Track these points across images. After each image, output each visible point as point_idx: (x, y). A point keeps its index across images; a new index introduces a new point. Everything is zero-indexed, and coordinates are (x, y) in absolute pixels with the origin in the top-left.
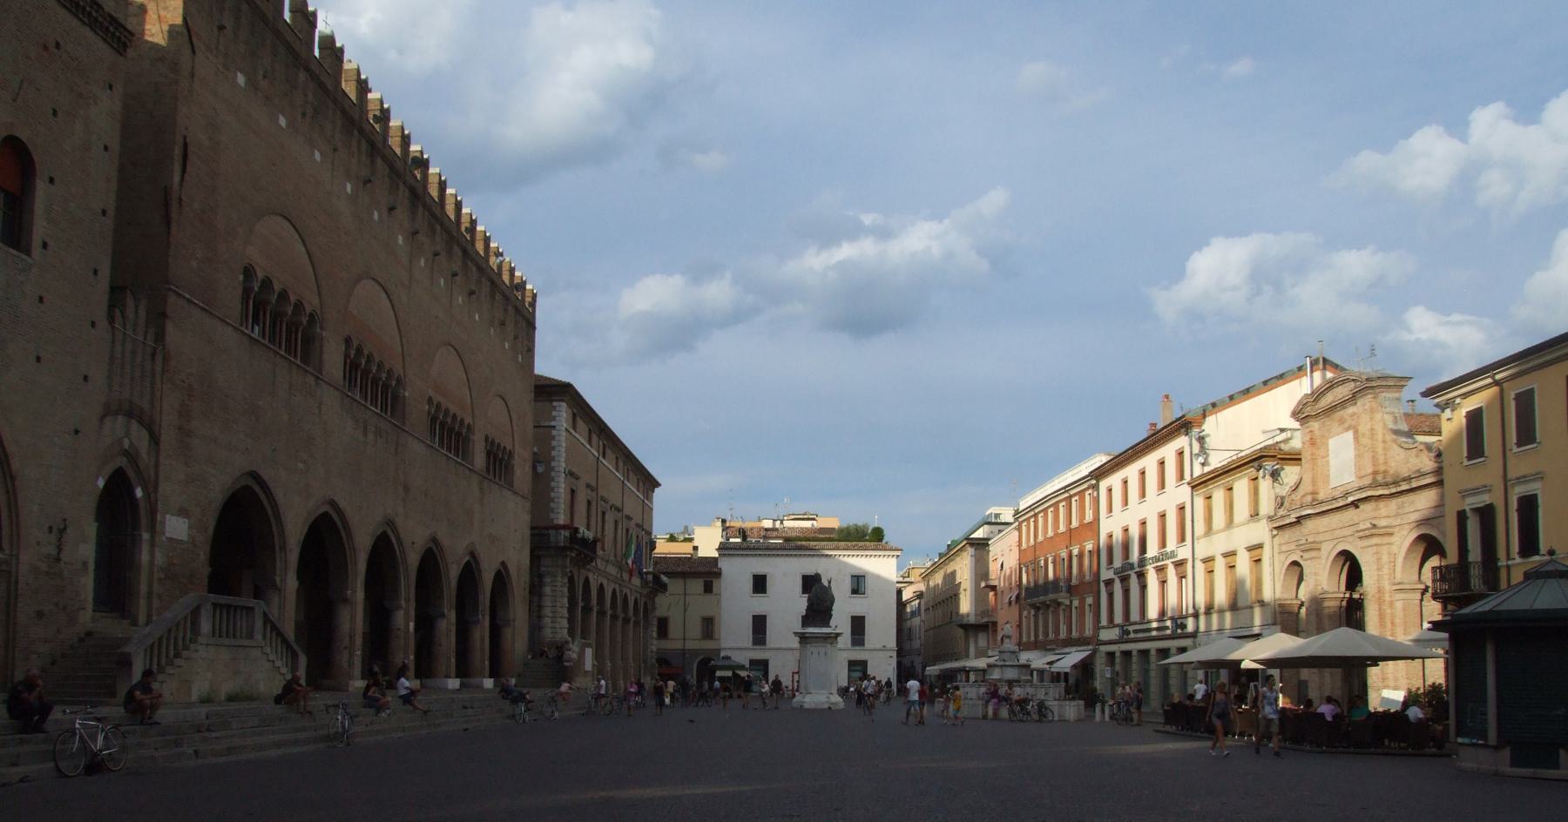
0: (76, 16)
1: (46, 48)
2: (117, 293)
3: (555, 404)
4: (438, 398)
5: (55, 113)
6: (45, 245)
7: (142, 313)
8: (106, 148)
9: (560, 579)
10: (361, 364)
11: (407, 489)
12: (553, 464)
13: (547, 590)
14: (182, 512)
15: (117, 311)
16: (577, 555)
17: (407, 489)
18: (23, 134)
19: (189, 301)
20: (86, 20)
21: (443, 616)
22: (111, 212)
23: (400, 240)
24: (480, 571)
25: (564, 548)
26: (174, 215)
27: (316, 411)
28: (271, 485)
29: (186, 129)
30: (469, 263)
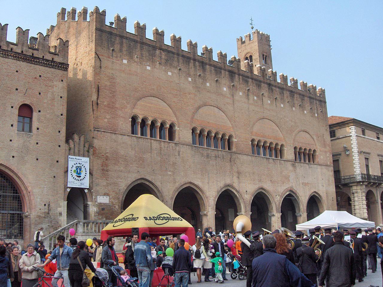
0: (47, 67)
1: (36, 78)
2: (69, 137)
3: (350, 127)
4: (257, 139)
5: (40, 94)
6: (38, 129)
7: (82, 139)
8: (61, 97)
9: (360, 194)
10: (205, 135)
11: (239, 173)
12: (353, 150)
13: (356, 199)
14: (105, 194)
15: (71, 141)
16: (368, 183)
17: (239, 173)
18: (27, 102)
19: (104, 132)
20: (51, 67)
21: (273, 215)
22: (65, 114)
23: (225, 89)
24: (297, 197)
25: (360, 182)
26: (95, 108)
27: (177, 154)
28: (153, 181)
29: (99, 83)
30: (274, 88)
